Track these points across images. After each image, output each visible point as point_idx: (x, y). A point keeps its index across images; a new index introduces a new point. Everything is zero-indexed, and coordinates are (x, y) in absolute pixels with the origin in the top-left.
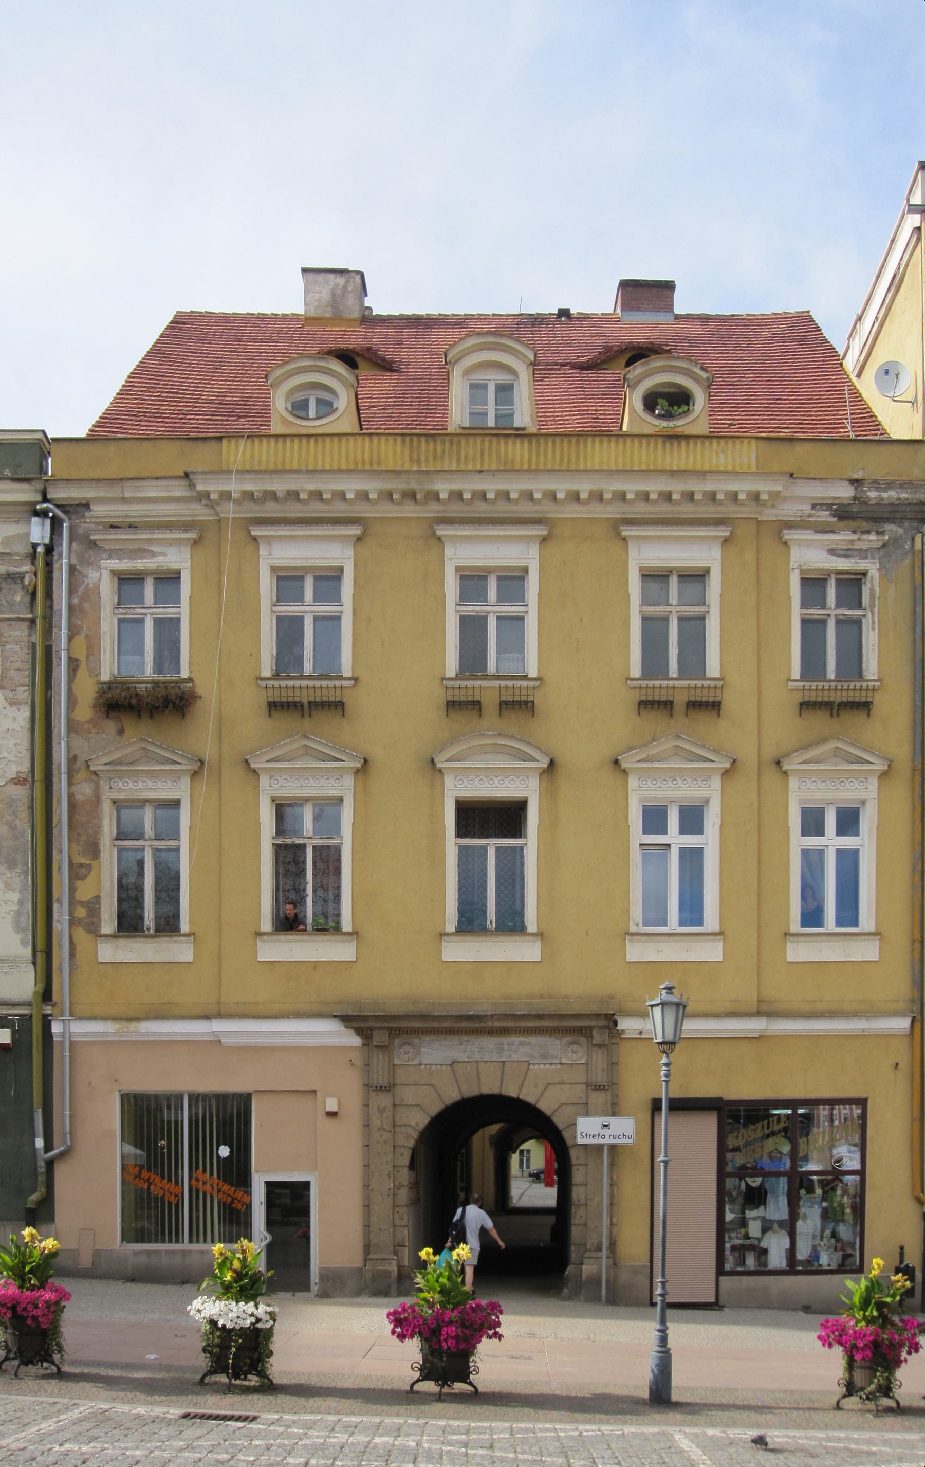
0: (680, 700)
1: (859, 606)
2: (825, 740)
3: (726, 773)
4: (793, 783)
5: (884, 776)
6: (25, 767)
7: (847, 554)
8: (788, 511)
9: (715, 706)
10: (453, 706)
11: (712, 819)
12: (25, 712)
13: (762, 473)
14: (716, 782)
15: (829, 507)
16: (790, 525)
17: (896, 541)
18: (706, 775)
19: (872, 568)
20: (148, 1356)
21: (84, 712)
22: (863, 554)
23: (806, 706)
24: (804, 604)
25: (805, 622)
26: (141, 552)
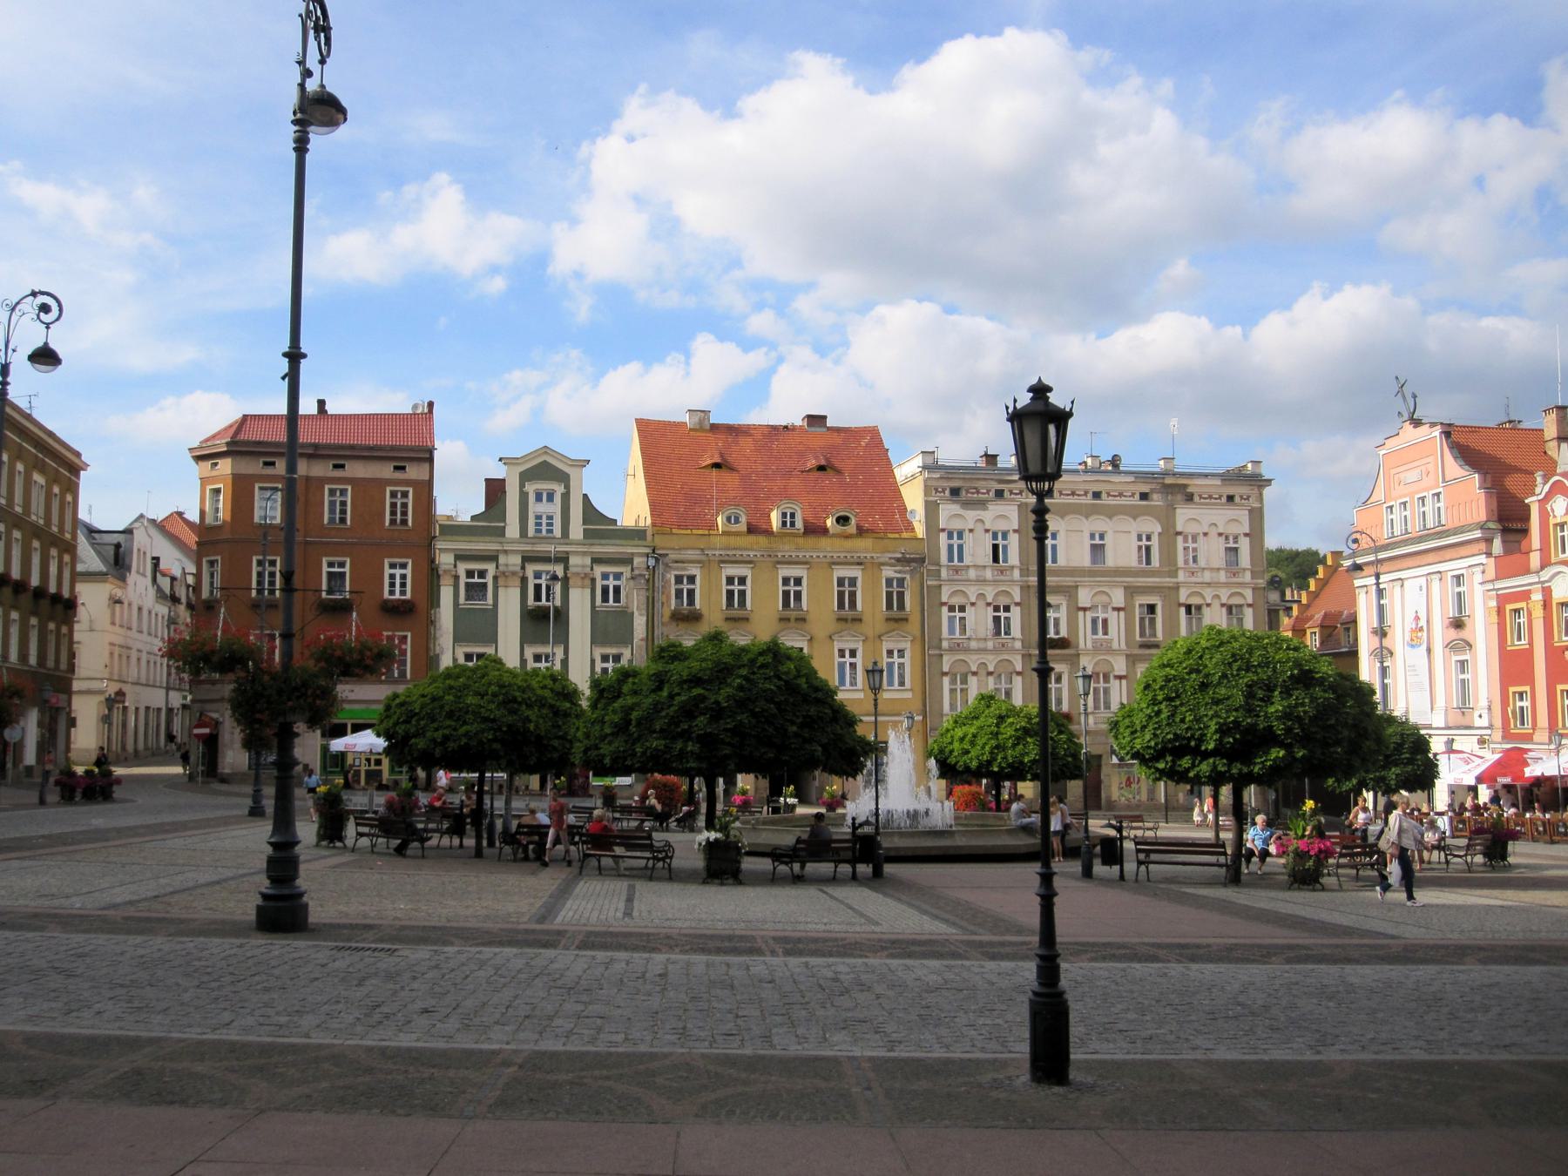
0: (850, 617)
1: (903, 587)
2: (894, 630)
3: (864, 641)
4: (884, 643)
5: (912, 641)
6: (645, 635)
7: (899, 572)
8: (882, 560)
9: (860, 620)
10: (781, 620)
11: (859, 654)
12: (645, 618)
13: (874, 551)
14: (861, 643)
15: (894, 558)
16: (883, 564)
17: (915, 568)
18: (858, 641)
19: (908, 577)
20: (721, 780)
21: (666, 618)
22: (905, 572)
23: (888, 620)
24: (887, 587)
25: (887, 592)
26: (684, 569)
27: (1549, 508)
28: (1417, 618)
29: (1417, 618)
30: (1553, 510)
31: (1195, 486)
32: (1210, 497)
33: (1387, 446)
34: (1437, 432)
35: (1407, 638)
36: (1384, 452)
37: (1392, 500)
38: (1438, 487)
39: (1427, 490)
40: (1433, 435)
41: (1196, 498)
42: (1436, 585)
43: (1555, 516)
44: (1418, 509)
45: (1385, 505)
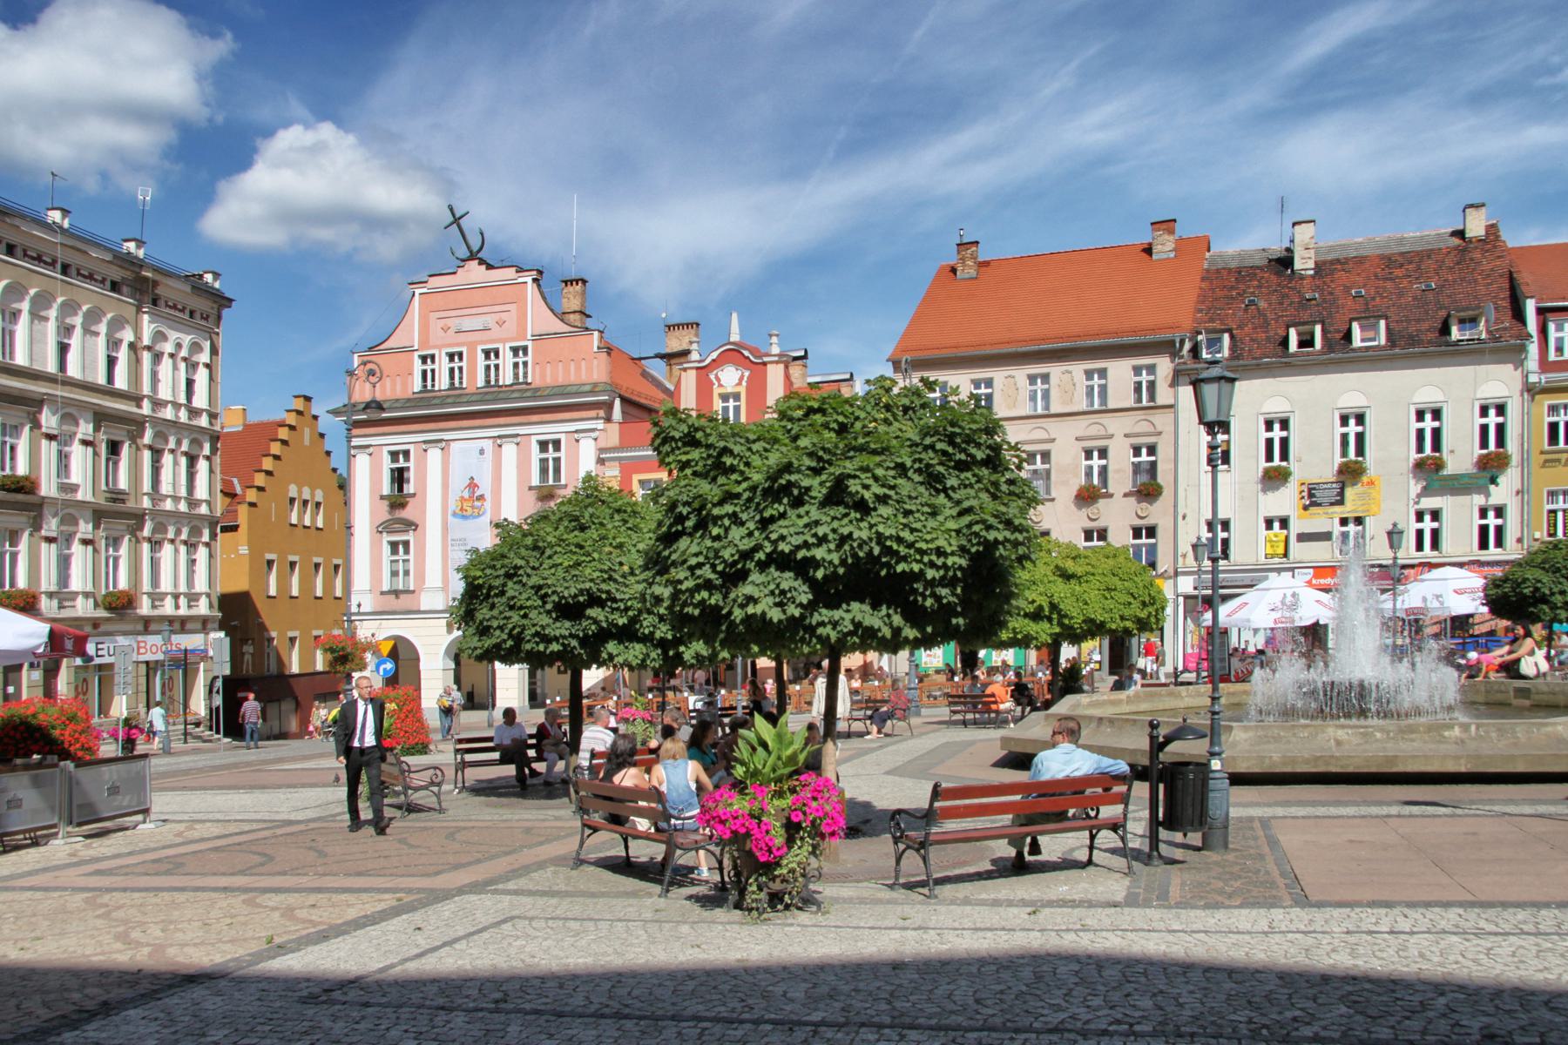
27: (712, 377)
28: (472, 485)
29: (472, 485)
30: (718, 379)
31: (171, 290)
32: (174, 307)
33: (428, 285)
34: (529, 280)
35: (453, 505)
36: (425, 290)
37: (435, 347)
38: (525, 338)
39: (504, 341)
40: (520, 280)
41: (162, 303)
42: (510, 450)
43: (720, 385)
44: (481, 361)
45: (416, 354)
